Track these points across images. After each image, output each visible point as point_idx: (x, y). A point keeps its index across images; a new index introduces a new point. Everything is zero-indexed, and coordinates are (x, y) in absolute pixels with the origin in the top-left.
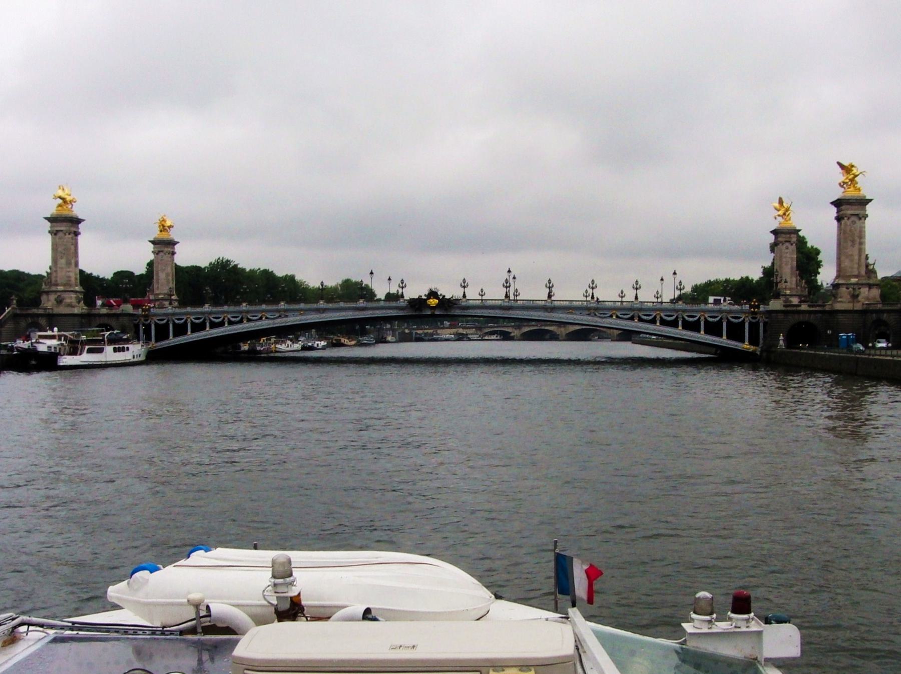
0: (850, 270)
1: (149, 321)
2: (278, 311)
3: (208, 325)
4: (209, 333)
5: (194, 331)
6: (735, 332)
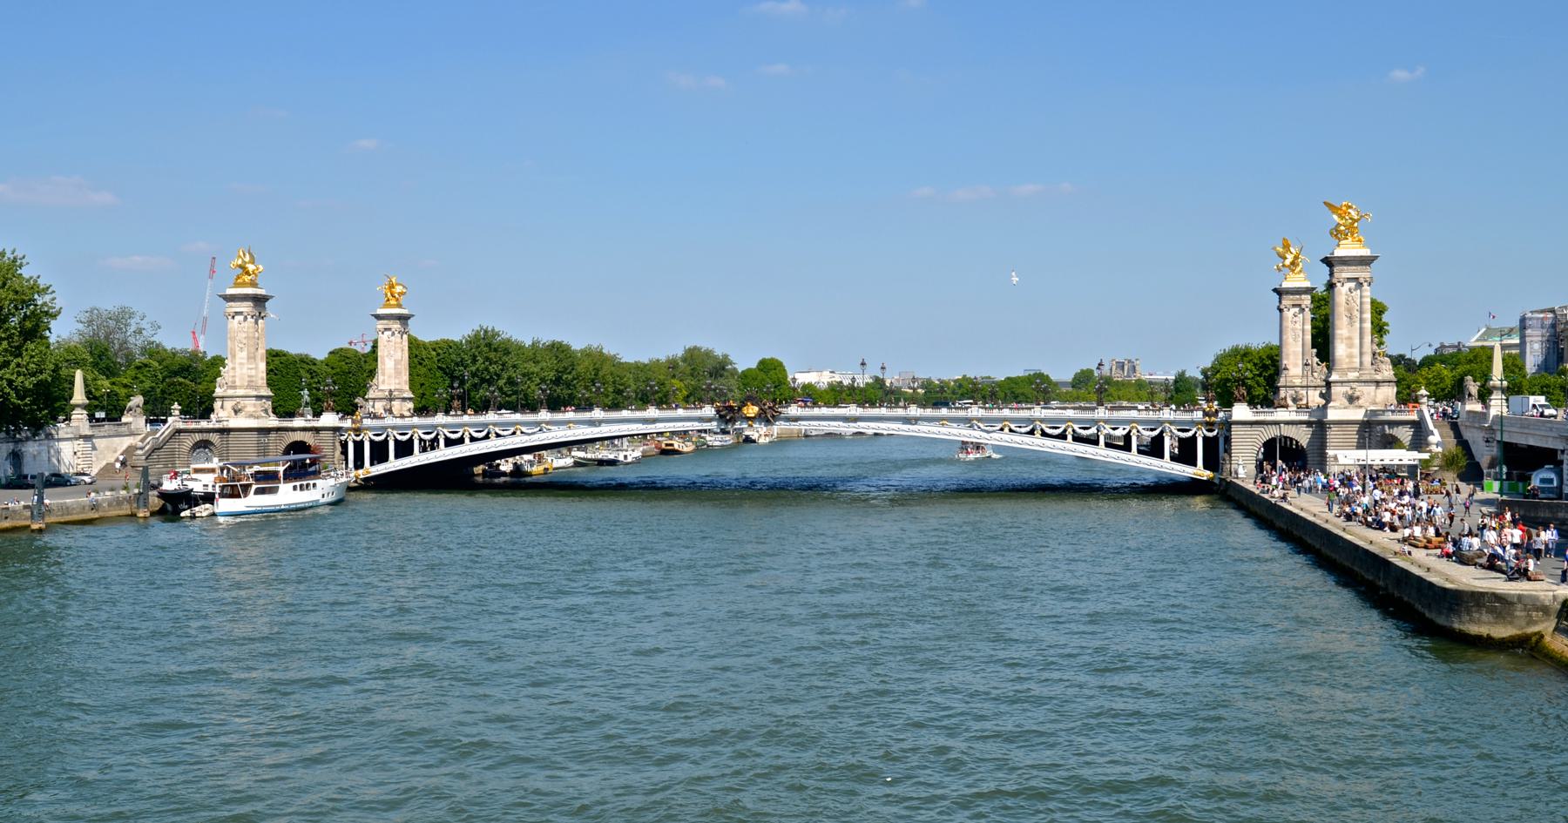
0: (1347, 360)
1: (361, 437)
2: (538, 424)
3: (442, 442)
4: (443, 454)
5: (424, 450)
6: (1185, 453)
